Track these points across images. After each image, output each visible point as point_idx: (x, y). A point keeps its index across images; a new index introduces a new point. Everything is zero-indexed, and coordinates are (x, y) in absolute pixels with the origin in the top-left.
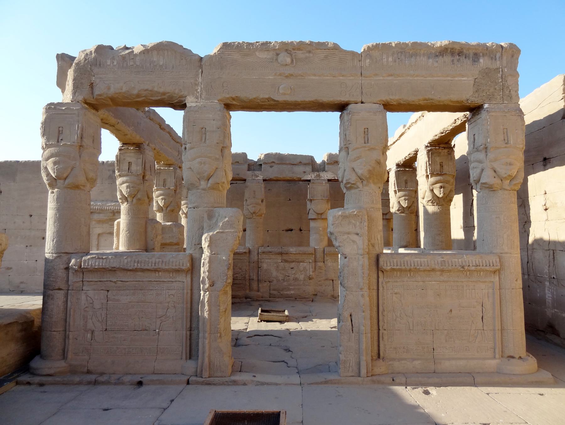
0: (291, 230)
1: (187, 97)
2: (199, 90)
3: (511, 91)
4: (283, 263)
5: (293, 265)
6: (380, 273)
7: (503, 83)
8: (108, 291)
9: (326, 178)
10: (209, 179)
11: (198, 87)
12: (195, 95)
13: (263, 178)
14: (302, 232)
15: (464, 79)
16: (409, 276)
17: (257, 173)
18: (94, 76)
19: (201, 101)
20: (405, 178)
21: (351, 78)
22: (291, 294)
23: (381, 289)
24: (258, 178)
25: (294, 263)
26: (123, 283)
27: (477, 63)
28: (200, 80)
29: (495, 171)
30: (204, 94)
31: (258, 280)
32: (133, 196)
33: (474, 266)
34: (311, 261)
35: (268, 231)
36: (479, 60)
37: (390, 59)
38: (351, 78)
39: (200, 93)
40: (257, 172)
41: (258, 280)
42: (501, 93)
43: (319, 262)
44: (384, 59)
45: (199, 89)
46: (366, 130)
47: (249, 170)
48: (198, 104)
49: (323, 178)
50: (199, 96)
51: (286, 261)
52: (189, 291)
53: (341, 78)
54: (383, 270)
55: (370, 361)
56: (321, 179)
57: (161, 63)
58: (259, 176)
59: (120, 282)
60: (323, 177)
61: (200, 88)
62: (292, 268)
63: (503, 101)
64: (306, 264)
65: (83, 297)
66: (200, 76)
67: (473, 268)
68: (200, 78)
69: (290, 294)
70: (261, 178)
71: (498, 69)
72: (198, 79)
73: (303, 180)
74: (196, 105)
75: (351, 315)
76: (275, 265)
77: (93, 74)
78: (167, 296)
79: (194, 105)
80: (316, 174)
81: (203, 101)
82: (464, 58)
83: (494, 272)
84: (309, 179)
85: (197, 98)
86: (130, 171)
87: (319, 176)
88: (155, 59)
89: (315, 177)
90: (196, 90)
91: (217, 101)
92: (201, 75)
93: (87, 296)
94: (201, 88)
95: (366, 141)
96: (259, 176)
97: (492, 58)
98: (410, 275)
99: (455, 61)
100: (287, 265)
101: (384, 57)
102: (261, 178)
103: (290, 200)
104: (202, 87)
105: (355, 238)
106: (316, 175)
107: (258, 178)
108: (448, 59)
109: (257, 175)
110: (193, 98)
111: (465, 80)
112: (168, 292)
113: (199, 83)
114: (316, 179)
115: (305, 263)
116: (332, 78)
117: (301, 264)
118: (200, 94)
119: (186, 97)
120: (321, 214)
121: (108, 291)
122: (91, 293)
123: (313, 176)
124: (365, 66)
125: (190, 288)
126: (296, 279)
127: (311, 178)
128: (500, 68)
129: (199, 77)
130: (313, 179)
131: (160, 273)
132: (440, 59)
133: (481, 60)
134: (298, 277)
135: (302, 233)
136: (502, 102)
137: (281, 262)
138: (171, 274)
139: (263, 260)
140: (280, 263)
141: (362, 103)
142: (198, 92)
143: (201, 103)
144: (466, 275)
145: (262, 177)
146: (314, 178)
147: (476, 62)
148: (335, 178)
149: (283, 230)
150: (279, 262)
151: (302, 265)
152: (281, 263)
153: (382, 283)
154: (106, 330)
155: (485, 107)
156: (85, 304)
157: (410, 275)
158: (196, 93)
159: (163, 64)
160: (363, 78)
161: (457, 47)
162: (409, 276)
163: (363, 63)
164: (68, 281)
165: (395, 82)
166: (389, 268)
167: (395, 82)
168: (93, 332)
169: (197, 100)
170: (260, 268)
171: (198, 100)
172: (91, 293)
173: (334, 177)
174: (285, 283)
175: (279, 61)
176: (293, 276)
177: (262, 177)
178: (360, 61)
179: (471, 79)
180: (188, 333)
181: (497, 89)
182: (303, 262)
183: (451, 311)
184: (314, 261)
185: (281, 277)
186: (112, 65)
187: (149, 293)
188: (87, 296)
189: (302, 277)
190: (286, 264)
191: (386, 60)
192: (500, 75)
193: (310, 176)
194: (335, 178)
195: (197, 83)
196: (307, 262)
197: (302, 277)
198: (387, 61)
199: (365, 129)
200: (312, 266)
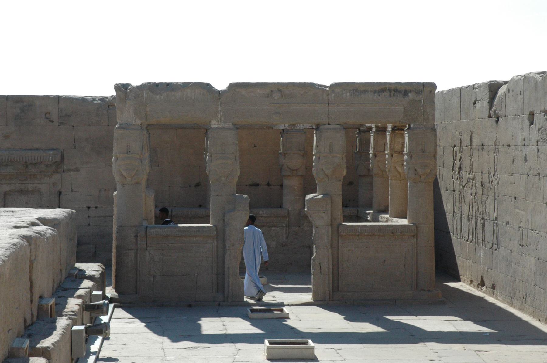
0: (257, 185)
2: (219, 116)
3: (429, 115)
7: (424, 110)
8: (163, 250)
14: (270, 187)
15: (397, 107)
16: (358, 238)
27: (406, 96)
29: (416, 170)
33: (400, 232)
36: (408, 94)
37: (348, 94)
39: (220, 118)
42: (422, 117)
44: (344, 94)
48: (219, 126)
50: (220, 120)
55: (331, 291)
56: (296, 128)
57: (193, 97)
61: (220, 115)
63: (423, 123)
64: (278, 229)
65: (147, 254)
66: (220, 106)
71: (420, 101)
75: (320, 264)
79: (216, 126)
82: (398, 93)
83: (413, 236)
85: (218, 122)
88: (189, 95)
90: (217, 116)
91: (232, 124)
92: (221, 106)
93: (150, 253)
94: (221, 115)
97: (417, 93)
98: (359, 238)
99: (392, 95)
101: (344, 93)
103: (255, 146)
108: (387, 94)
111: (397, 108)
114: (290, 128)
115: (278, 227)
117: (273, 228)
119: (210, 122)
121: (163, 250)
122: (152, 252)
124: (331, 99)
128: (422, 100)
130: (287, 129)
131: (197, 238)
132: (382, 94)
133: (409, 94)
136: (422, 123)
141: (329, 124)
142: (219, 118)
143: (221, 125)
144: (395, 237)
146: (287, 128)
147: (406, 95)
149: (246, 186)
154: (163, 275)
155: (411, 127)
157: (359, 238)
158: (217, 118)
159: (195, 99)
161: (393, 87)
162: (358, 238)
163: (329, 97)
164: (137, 244)
169: (218, 123)
173: (311, 126)
175: (273, 96)
178: (328, 95)
179: (402, 107)
180: (216, 276)
181: (420, 114)
182: (276, 227)
183: (385, 261)
188: (150, 253)
191: (345, 95)
192: (422, 105)
194: (311, 126)
196: (280, 226)
198: (346, 96)
199: (330, 142)
200: (286, 230)
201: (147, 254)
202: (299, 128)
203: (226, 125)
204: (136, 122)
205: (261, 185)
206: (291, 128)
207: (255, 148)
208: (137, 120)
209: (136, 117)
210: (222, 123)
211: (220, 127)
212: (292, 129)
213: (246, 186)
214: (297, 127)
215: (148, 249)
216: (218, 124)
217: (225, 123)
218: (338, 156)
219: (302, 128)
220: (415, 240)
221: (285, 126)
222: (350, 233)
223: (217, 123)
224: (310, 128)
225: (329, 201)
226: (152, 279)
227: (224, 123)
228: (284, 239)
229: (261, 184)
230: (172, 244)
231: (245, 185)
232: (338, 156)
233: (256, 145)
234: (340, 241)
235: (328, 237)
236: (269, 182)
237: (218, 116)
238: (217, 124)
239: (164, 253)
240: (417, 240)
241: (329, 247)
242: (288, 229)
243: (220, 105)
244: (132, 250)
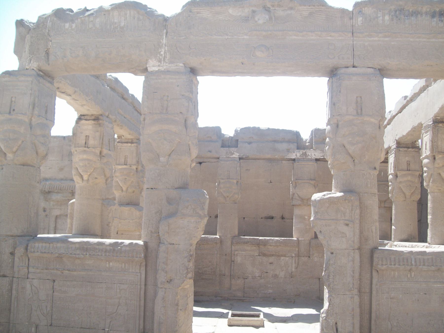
0: (272, 218)
1: (149, 60)
2: (162, 53)
4: (261, 257)
5: (271, 259)
6: (374, 273)
9: (314, 157)
10: (170, 154)
11: (161, 49)
12: (158, 58)
13: (239, 156)
14: (284, 220)
16: (409, 275)
17: (232, 149)
18: (51, 41)
19: (164, 65)
20: (407, 159)
21: (341, 38)
22: (269, 294)
23: (374, 292)
24: (234, 156)
25: (273, 257)
26: (70, 272)
28: (164, 41)
30: (168, 56)
31: (231, 275)
32: (89, 174)
34: (294, 255)
35: (244, 218)
38: (341, 38)
39: (163, 55)
40: (233, 149)
41: (231, 275)
43: (303, 257)
45: (162, 51)
46: (359, 99)
48: (161, 68)
49: (310, 157)
50: (163, 59)
51: (264, 255)
52: (143, 287)
53: (329, 38)
54: (378, 270)
56: (307, 158)
58: (234, 154)
59: (67, 272)
60: (310, 155)
61: (163, 50)
62: (271, 263)
64: (287, 258)
65: (28, 286)
66: (165, 37)
68: (164, 39)
69: (268, 293)
70: (236, 156)
72: (161, 41)
73: (286, 159)
74: (159, 69)
76: (251, 259)
77: (50, 39)
78: (118, 291)
79: (156, 69)
80: (301, 152)
81: (166, 64)
84: (293, 157)
85: (160, 61)
86: (86, 146)
87: (305, 154)
89: (300, 156)
91: (183, 65)
92: (166, 36)
94: (165, 50)
96: (234, 154)
98: (411, 275)
100: (265, 259)
102: (236, 155)
103: (271, 182)
104: (166, 49)
106: (301, 153)
107: (234, 156)
109: (233, 152)
110: (155, 62)
112: (119, 286)
113: (162, 44)
115: (287, 257)
116: (319, 38)
117: (282, 258)
118: (163, 57)
121: (54, 281)
122: (36, 282)
123: (298, 155)
125: (143, 283)
126: (276, 276)
127: (296, 157)
129: (163, 38)
134: (278, 274)
135: (285, 221)
137: (258, 256)
138: (123, 265)
139: (236, 253)
140: (256, 257)
142: (162, 55)
143: (165, 66)
145: (238, 154)
146: (299, 157)
148: (324, 157)
149: (262, 218)
150: (256, 256)
151: (283, 259)
152: (258, 257)
153: (376, 285)
156: (30, 294)
158: (158, 56)
160: (355, 39)
162: (409, 275)
165: (393, 43)
167: (393, 43)
169: (159, 63)
170: (233, 261)
171: (161, 64)
172: (36, 282)
173: (323, 156)
174: (262, 281)
176: (272, 272)
177: (238, 154)
184: (297, 256)
185: (258, 273)
186: (70, 28)
187: (99, 286)
189: (282, 274)
190: (264, 258)
193: (294, 154)
195: (161, 44)
196: (289, 257)
197: (282, 274)
199: (357, 97)
201: (28, 286)
202: (311, 158)
203: (172, 67)
204: (30, 65)
205: (276, 218)
206: (302, 158)
207: (271, 183)
208: (32, 62)
209: (31, 56)
210: (166, 63)
211: (163, 69)
212: (304, 159)
213: (262, 218)
214: (309, 156)
215: (30, 276)
216: (159, 66)
217: (171, 62)
218: (372, 120)
219: (314, 158)
222: (395, 265)
223: (158, 64)
224: (321, 158)
225: (357, 203)
227: (169, 63)
228: (293, 270)
229: (276, 217)
230: (69, 270)
231: (261, 218)
232: (372, 120)
233: (272, 181)
235: (353, 271)
236: (283, 216)
237: (161, 52)
238: (157, 65)
239: (55, 287)
241: (356, 292)
242: (297, 259)
243: (165, 35)
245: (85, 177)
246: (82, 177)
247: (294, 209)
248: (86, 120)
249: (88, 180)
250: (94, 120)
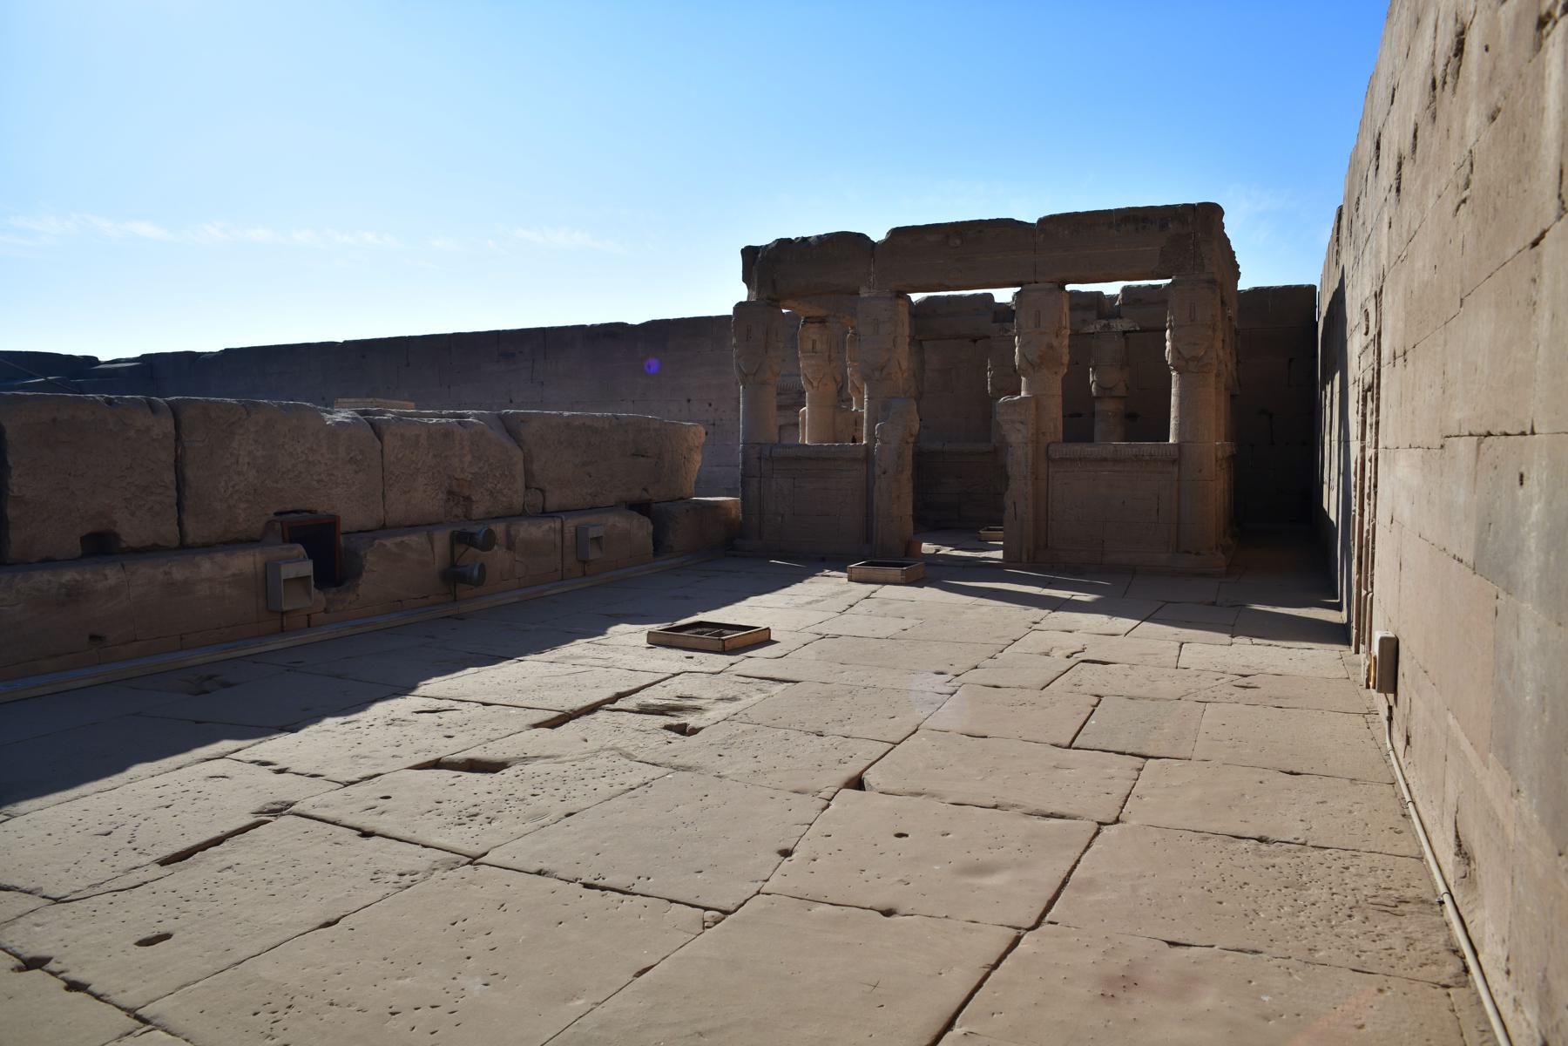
37: (1066, 232)
47: (994, 322)
67: (1148, 458)
79: (866, 295)
84: (1091, 331)
85: (870, 288)
95: (1037, 325)
105: (1020, 427)
120: (1111, 389)
123: (1098, 327)
133: (1170, 226)
141: (1036, 283)
166: (1057, 457)
168: (783, 516)
192: (1191, 242)
193: (1093, 327)
215: (775, 476)
220: (1176, 469)
221: (1096, 328)
226: (780, 519)
234: (1050, 470)
240: (1179, 469)
244: (754, 477)
245: (815, 384)
246: (811, 383)
247: (1096, 404)
248: (812, 323)
249: (818, 387)
250: (820, 322)
